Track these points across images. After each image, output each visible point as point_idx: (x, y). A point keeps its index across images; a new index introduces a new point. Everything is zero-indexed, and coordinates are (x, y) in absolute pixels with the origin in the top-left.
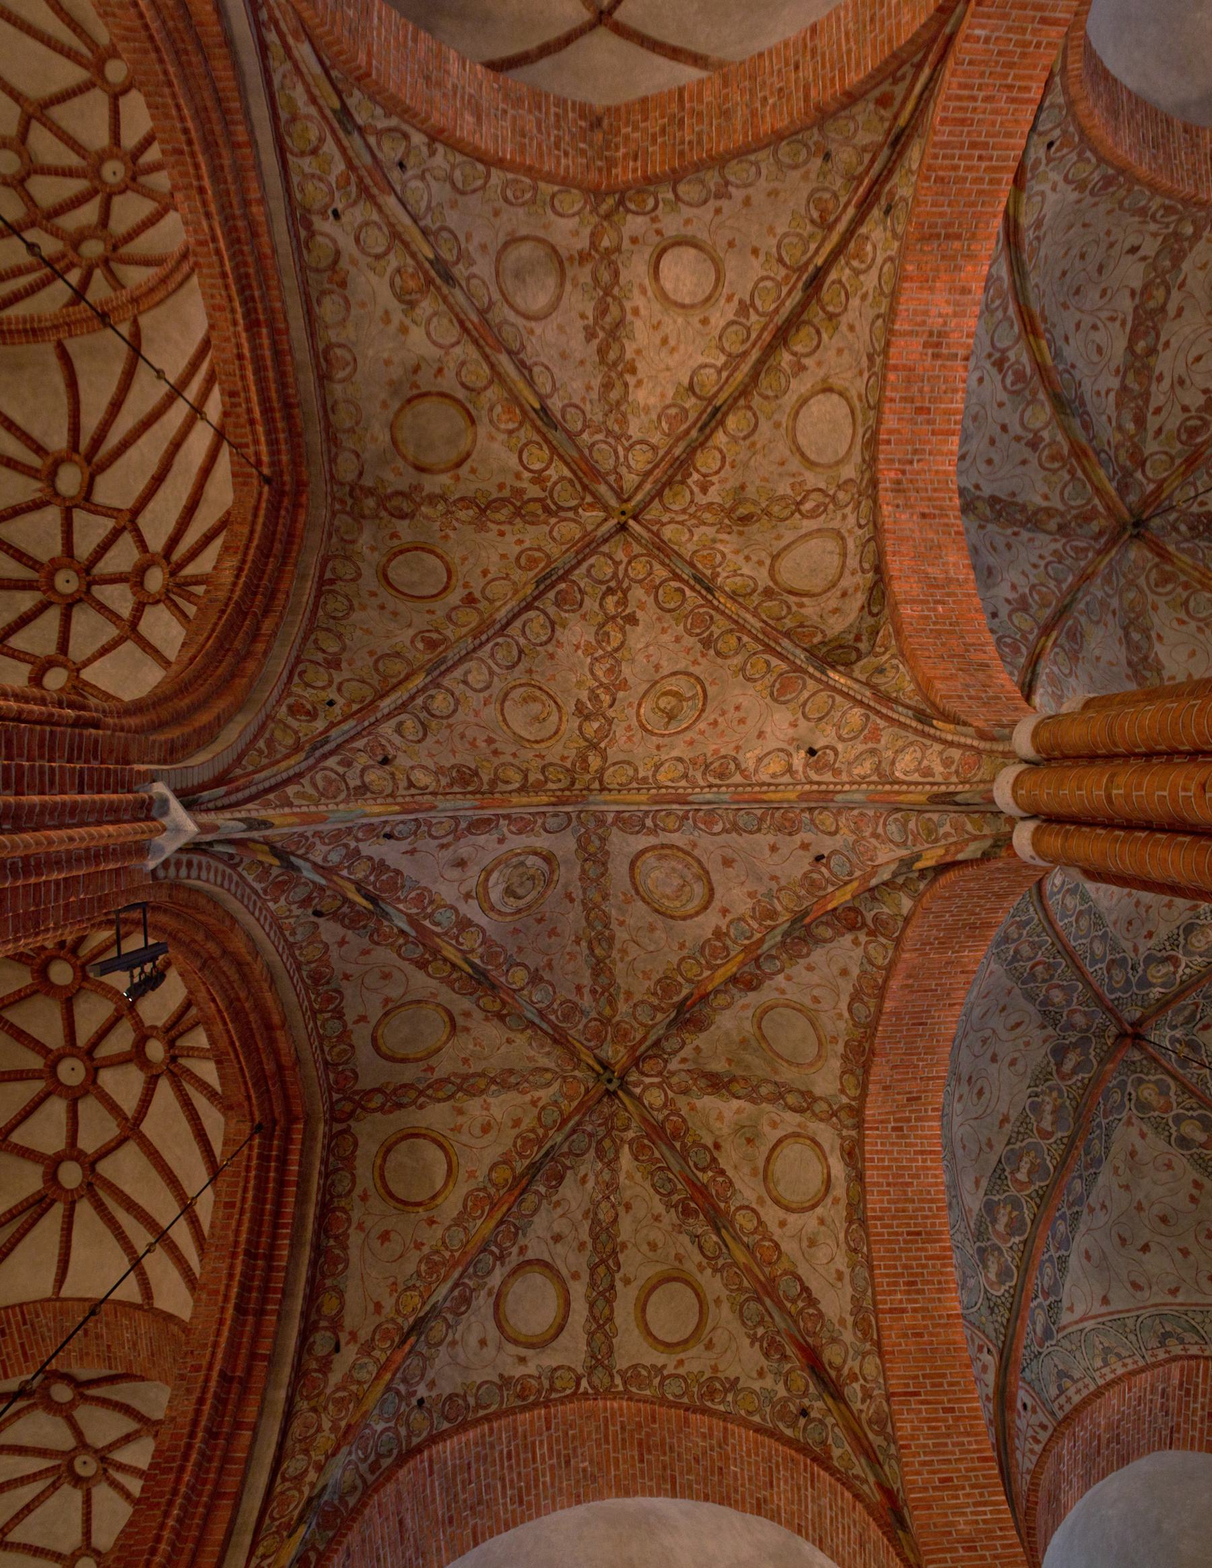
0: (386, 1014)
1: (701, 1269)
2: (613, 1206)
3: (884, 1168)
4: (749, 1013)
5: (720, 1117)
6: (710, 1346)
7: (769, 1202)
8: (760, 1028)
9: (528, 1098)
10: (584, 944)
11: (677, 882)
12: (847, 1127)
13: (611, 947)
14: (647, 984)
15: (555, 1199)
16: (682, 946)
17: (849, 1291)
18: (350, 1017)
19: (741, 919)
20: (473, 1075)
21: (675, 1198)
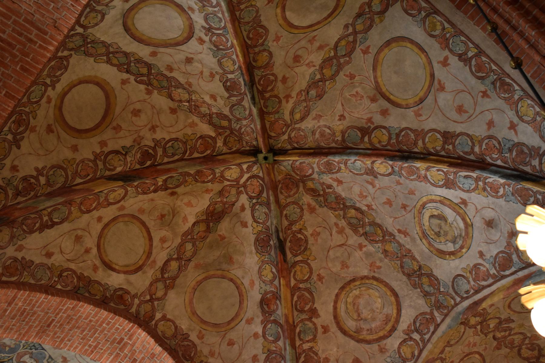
0: (432, 76)
1: (103, 144)
2: (181, 101)
3: (103, 322)
4: (246, 282)
5: (189, 204)
6: (50, 130)
7: (118, 214)
8: (231, 280)
9: (294, 94)
10: (365, 208)
11: (365, 313)
12: (139, 306)
13: (350, 224)
14: (310, 231)
15: (217, 77)
16: (320, 278)
17: (37, 260)
18: (454, 61)
19: (314, 339)
20: (337, 72)
21: (160, 152)
